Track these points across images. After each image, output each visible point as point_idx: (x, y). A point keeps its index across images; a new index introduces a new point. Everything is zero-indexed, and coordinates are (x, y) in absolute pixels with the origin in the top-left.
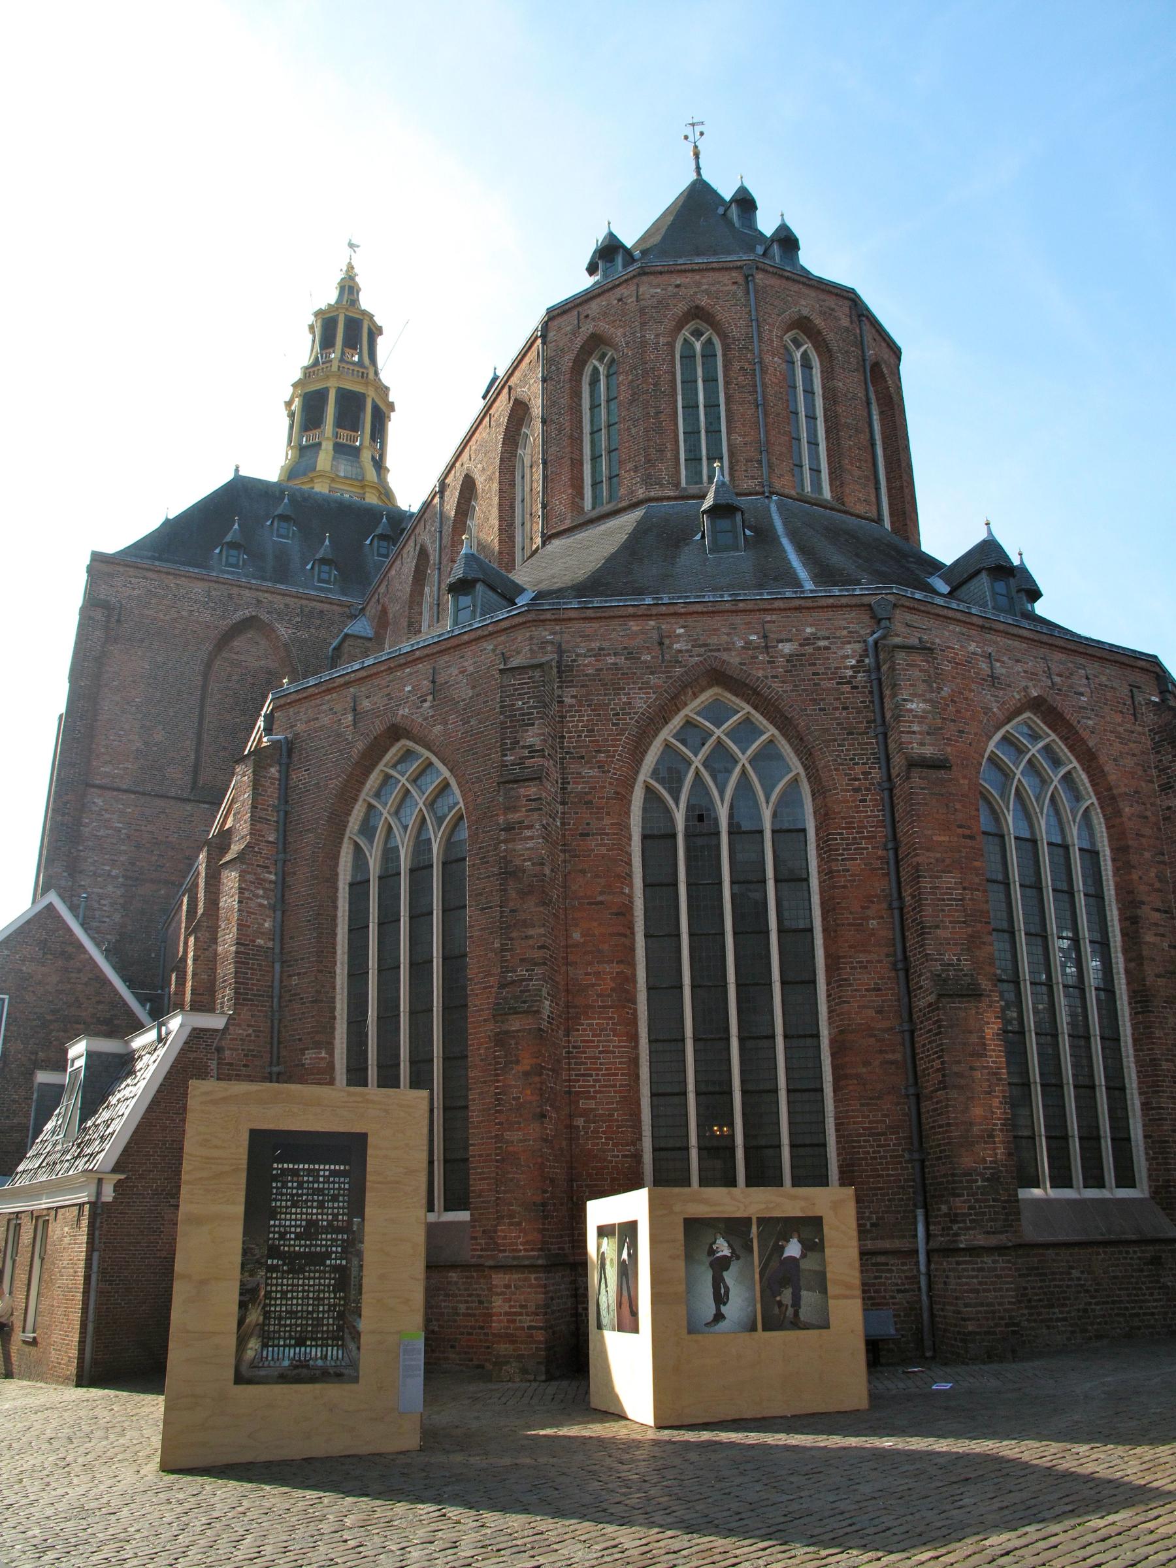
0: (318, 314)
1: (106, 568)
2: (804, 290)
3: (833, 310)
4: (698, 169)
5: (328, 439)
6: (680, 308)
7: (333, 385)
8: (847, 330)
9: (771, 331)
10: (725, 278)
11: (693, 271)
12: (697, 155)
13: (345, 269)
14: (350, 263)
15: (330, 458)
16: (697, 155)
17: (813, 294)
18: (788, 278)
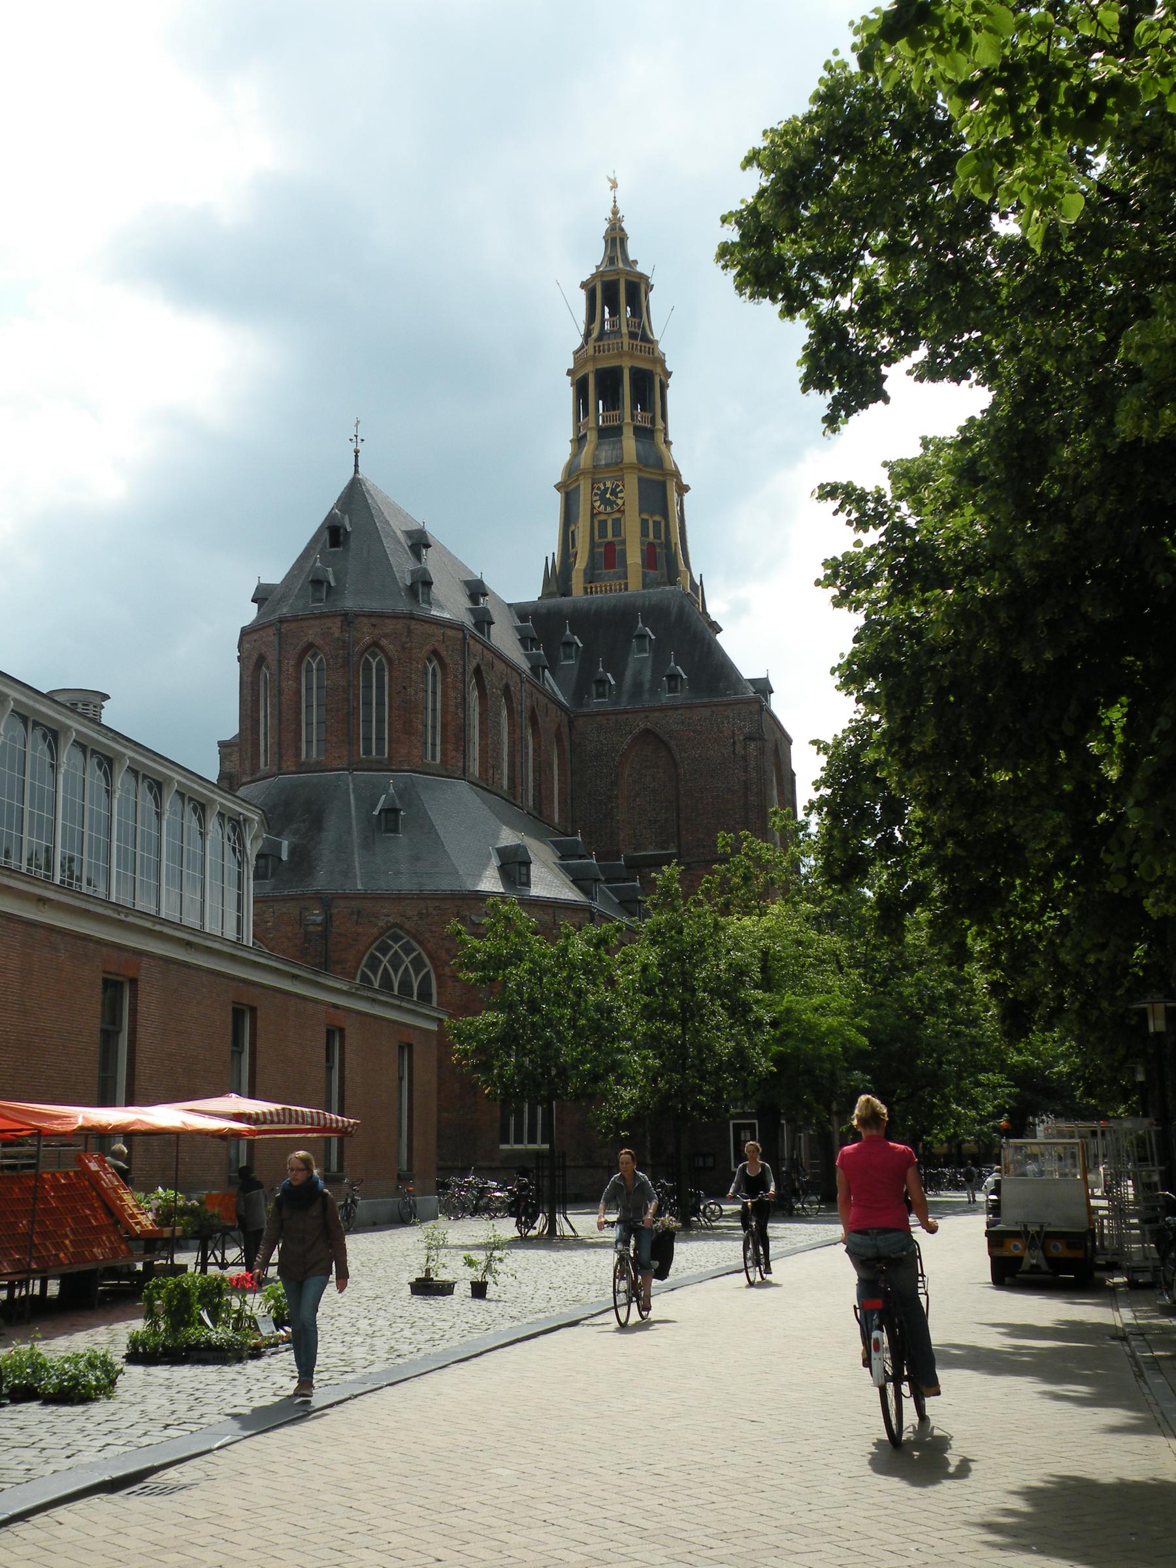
0: (583, 285)
1: (228, 750)
2: (312, 622)
3: (330, 628)
4: (356, 465)
5: (591, 428)
6: (255, 656)
7: (589, 369)
8: (338, 639)
9: (288, 663)
10: (271, 631)
11: (260, 629)
12: (357, 452)
14: (615, 206)
15: (593, 446)
16: (357, 452)
17: (317, 622)
18: (301, 619)
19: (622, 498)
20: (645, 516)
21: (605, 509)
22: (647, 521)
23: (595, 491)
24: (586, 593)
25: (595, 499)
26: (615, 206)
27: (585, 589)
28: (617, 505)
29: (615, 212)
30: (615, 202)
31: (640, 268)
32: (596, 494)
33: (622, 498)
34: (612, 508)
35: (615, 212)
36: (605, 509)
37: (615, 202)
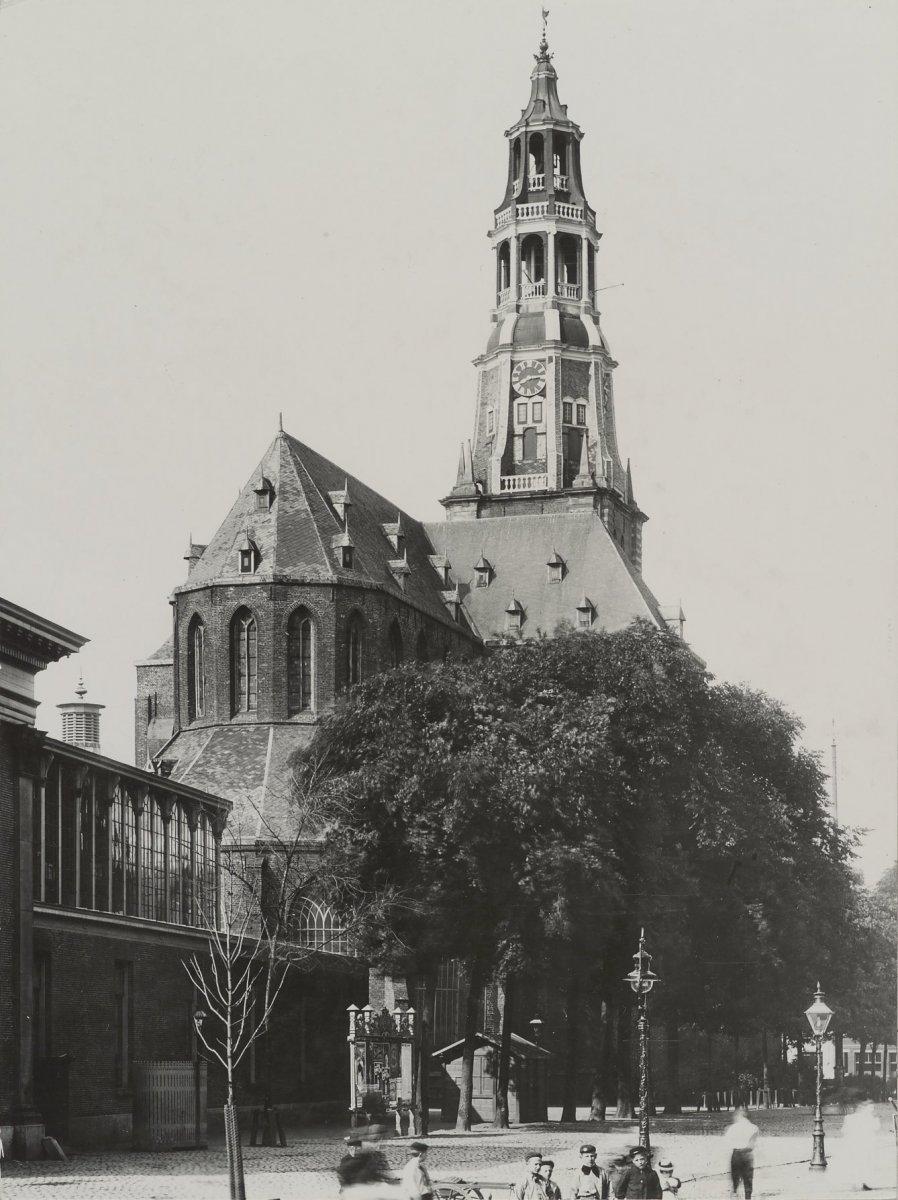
13: (538, 52)
14: (544, 40)
19: (544, 380)
20: (568, 399)
21: (526, 392)
22: (571, 404)
23: (515, 371)
24: (503, 487)
25: (514, 379)
26: (544, 40)
27: (503, 482)
28: (538, 387)
29: (544, 48)
30: (544, 35)
31: (571, 116)
32: (516, 375)
33: (544, 380)
34: (533, 391)
35: (544, 48)
36: (526, 392)
37: (544, 35)
